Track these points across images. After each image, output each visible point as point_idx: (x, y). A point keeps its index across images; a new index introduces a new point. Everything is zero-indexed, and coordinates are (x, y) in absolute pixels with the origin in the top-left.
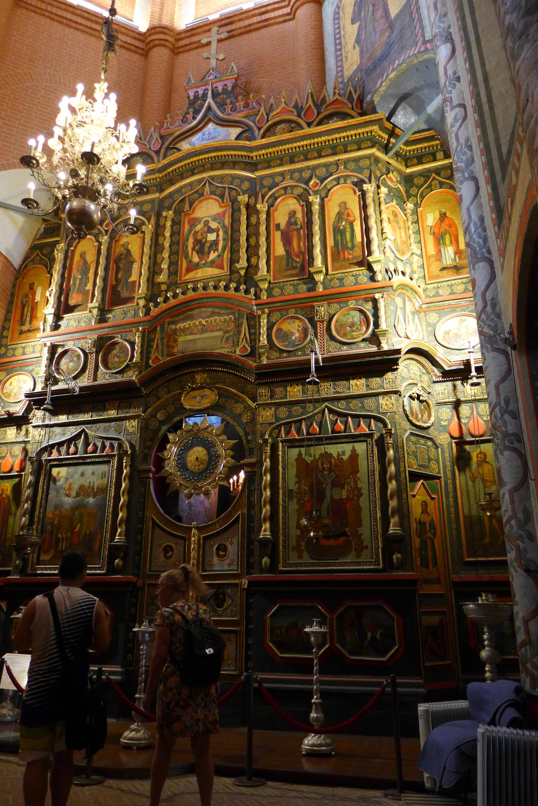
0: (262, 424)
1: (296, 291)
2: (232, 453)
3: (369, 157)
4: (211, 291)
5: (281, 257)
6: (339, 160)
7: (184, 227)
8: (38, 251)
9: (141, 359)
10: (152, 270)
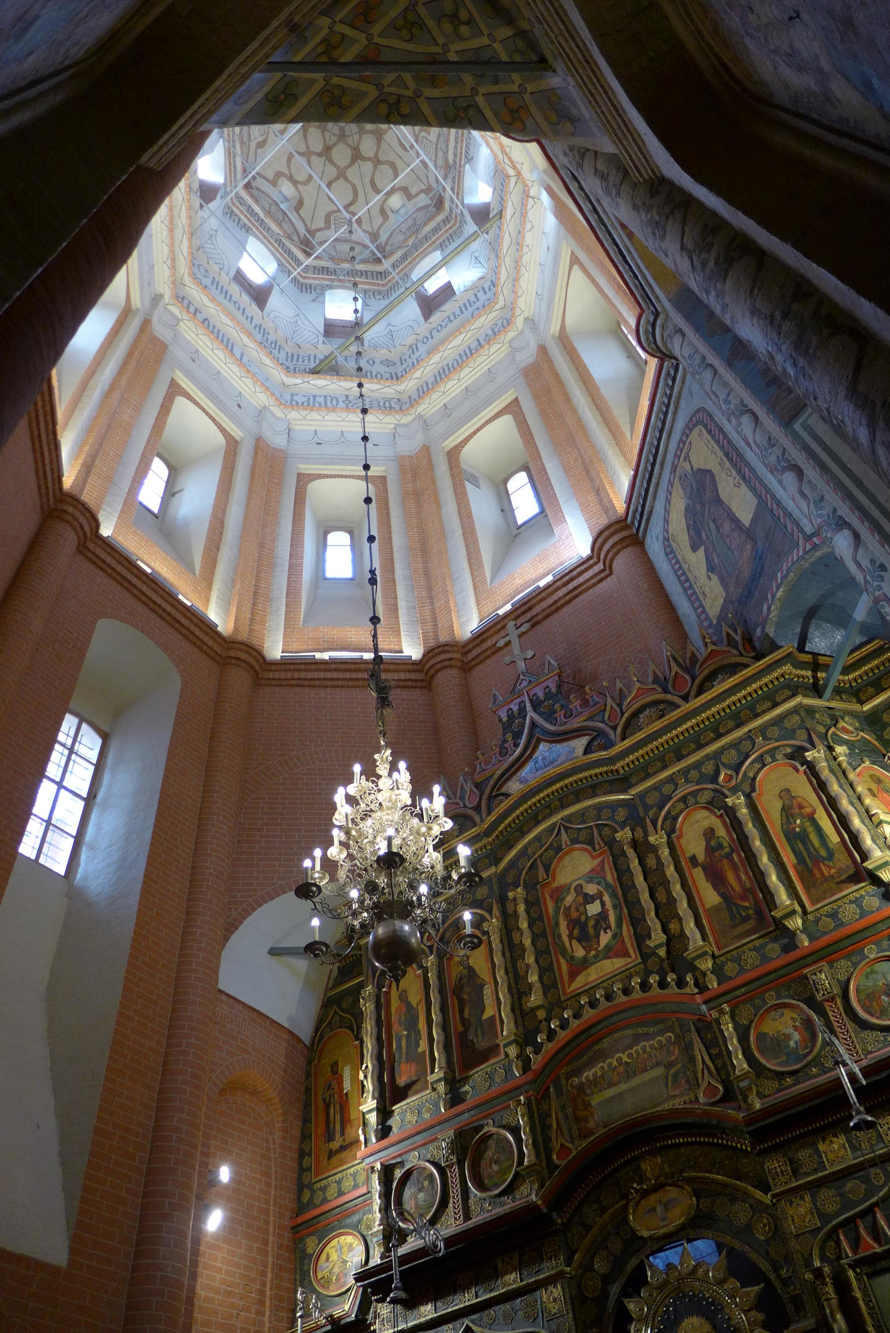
0: (797, 1236)
1: (765, 959)
2: (760, 1317)
3: (795, 711)
4: (622, 999)
5: (717, 908)
6: (750, 731)
7: (546, 905)
8: (335, 1006)
9: (537, 1155)
10: (515, 991)
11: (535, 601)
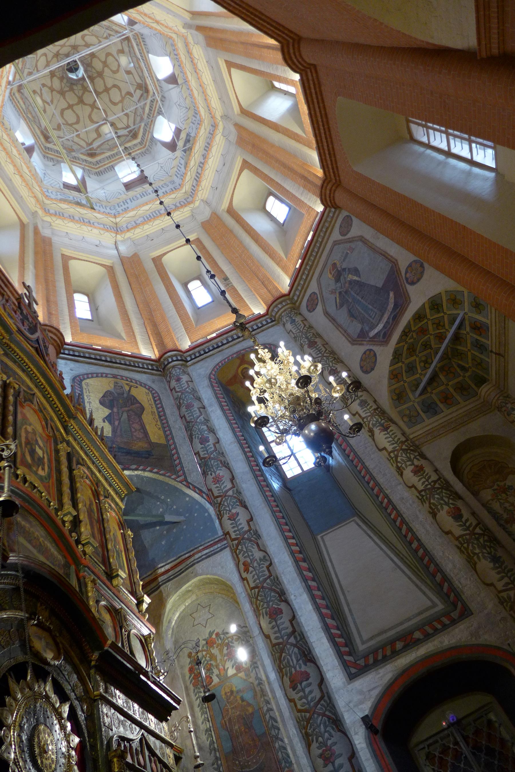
11: (11, 289)
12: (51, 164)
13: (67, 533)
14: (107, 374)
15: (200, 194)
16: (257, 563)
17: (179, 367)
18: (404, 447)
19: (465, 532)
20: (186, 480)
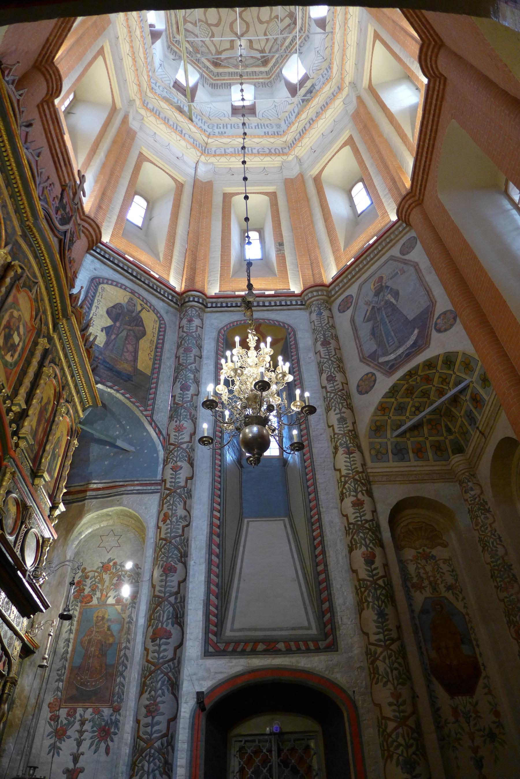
11: (69, 170)
12: (172, 57)
13: (7, 422)
14: (126, 287)
15: (297, 149)
16: (176, 519)
17: (197, 309)
18: (357, 477)
19: (369, 578)
20: (151, 416)
